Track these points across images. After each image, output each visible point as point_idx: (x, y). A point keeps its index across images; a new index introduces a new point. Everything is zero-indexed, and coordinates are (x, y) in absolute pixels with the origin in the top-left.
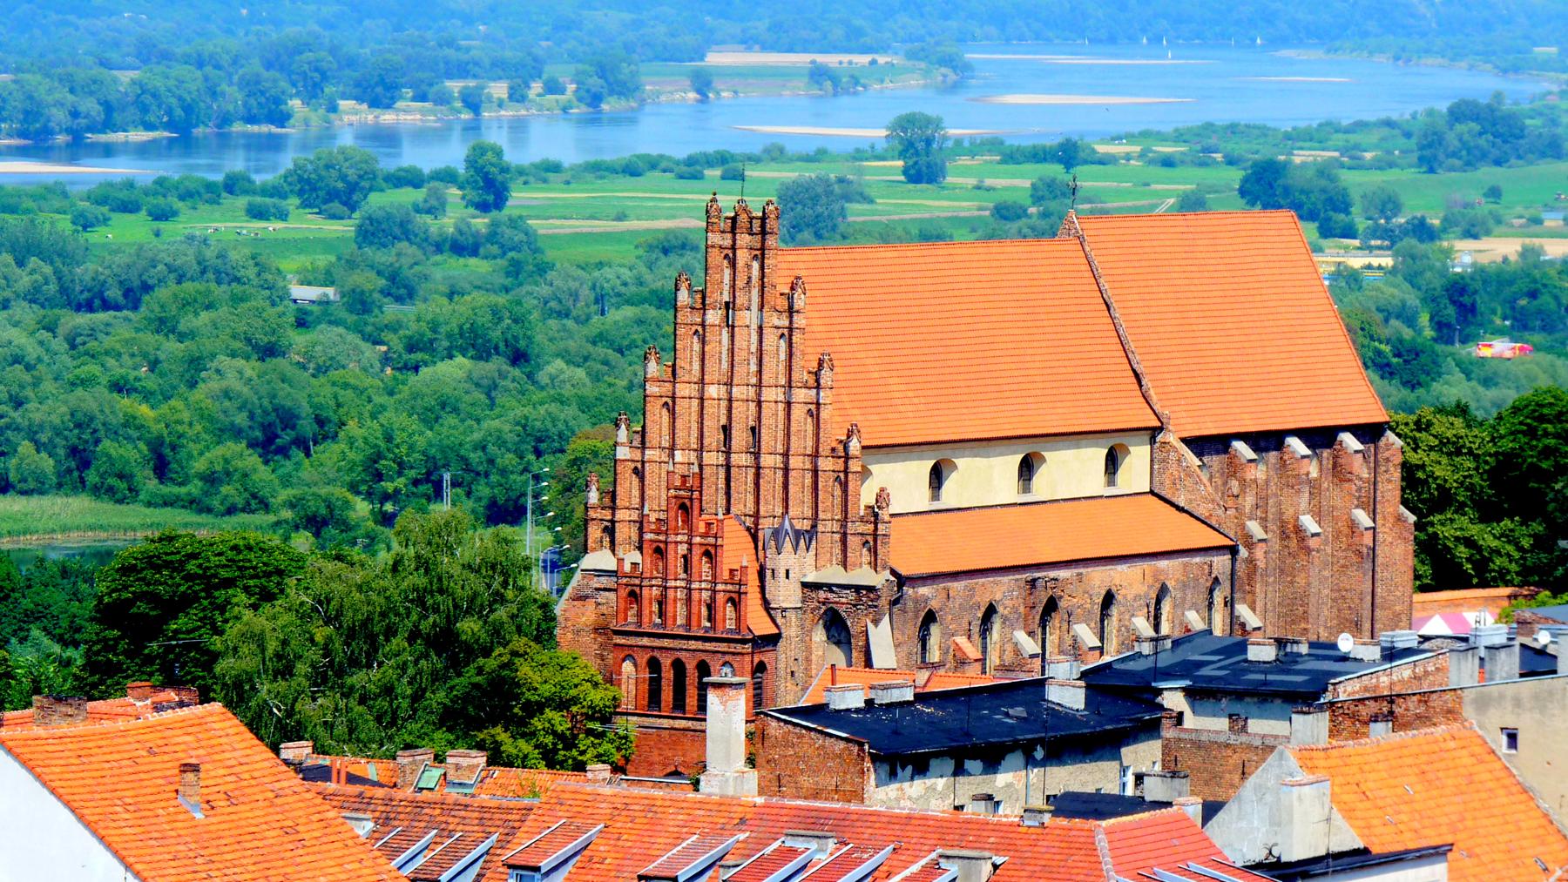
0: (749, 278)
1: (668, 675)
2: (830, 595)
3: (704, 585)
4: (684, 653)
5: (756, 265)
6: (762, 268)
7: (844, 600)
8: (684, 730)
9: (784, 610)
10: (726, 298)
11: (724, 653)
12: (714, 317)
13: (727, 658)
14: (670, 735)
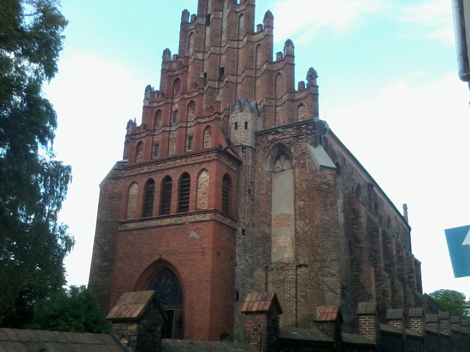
2: (276, 136)
4: (172, 171)
7: (288, 136)
9: (244, 147)
10: (209, 12)
13: (204, 166)
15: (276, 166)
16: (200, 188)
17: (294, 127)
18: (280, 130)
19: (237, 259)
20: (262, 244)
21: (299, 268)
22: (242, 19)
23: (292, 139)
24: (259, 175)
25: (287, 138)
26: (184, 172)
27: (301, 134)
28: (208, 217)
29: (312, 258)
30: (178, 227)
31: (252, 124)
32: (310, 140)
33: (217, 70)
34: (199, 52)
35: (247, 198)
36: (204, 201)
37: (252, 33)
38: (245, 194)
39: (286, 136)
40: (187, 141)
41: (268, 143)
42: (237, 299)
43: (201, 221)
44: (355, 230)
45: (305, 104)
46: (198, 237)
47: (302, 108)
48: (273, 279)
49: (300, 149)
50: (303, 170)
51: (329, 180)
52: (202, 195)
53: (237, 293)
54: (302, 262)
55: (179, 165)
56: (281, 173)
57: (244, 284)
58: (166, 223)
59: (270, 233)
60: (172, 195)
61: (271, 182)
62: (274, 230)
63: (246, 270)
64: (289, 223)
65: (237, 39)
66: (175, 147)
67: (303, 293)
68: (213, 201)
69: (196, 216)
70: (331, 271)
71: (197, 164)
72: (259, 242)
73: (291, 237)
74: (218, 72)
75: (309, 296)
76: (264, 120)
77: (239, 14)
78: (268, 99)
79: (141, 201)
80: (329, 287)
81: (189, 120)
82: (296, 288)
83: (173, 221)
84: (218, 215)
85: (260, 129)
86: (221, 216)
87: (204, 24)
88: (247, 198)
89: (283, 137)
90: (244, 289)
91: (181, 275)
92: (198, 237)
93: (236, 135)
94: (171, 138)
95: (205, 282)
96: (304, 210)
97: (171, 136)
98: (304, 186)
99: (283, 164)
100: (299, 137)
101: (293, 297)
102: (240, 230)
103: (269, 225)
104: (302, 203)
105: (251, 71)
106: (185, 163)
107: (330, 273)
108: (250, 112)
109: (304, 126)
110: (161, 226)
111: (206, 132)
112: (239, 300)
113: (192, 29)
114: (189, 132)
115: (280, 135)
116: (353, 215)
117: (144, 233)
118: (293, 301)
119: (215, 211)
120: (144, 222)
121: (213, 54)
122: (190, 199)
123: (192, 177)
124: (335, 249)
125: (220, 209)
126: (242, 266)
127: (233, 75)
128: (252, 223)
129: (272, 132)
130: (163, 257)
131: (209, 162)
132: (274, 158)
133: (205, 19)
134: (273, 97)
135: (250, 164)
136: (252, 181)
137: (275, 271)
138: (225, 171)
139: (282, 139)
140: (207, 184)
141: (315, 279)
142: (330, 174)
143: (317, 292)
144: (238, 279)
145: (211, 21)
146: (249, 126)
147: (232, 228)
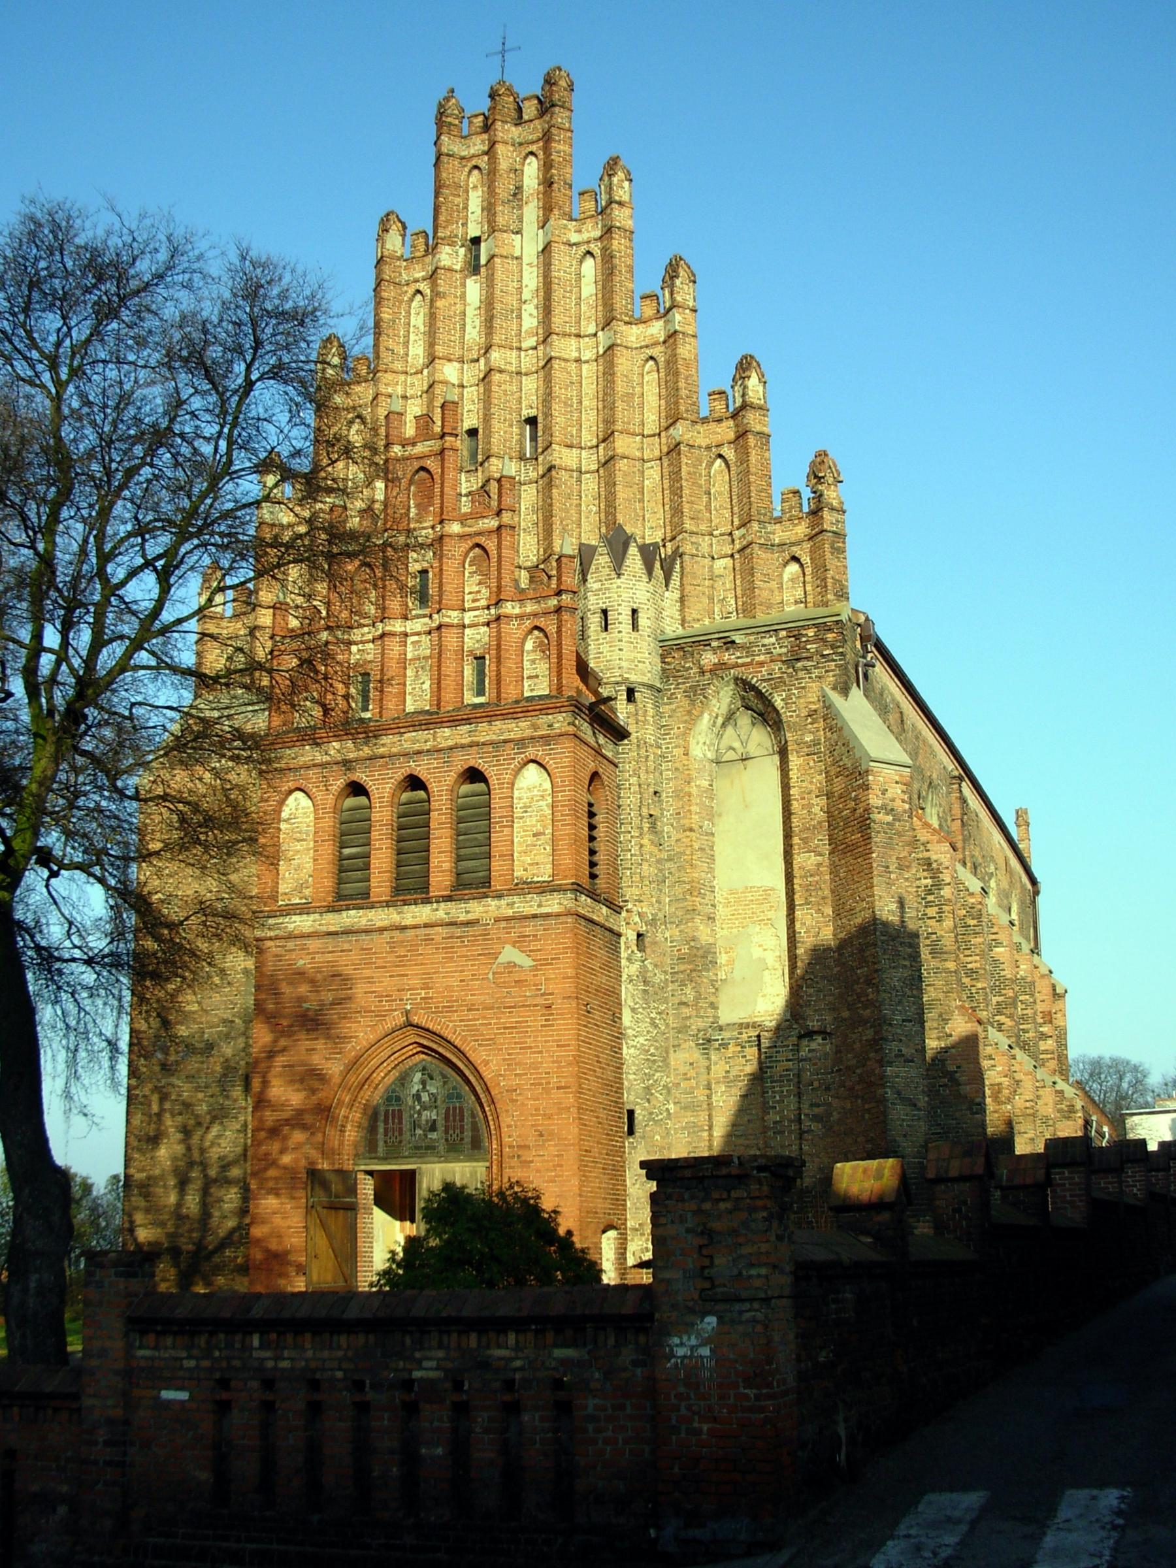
0: (519, 189)
1: (383, 815)
2: (728, 657)
3: (468, 618)
4: (424, 760)
5: (531, 171)
6: (547, 165)
7: (762, 658)
8: (426, 926)
10: (473, 231)
11: (521, 743)
12: (452, 257)
13: (531, 752)
14: (393, 945)
15: (725, 743)
16: (521, 818)
17: (783, 633)
18: (738, 638)
19: (627, 1018)
20: (694, 974)
21: (805, 1042)
22: (589, 266)
23: (776, 666)
24: (677, 769)
25: (761, 664)
26: (466, 767)
27: (804, 655)
28: (554, 904)
29: (846, 1014)
30: (458, 931)
31: (651, 613)
32: (831, 674)
33: (511, 426)
34: (450, 360)
35: (645, 841)
36: (538, 859)
37: (627, 319)
38: (642, 828)
39: (757, 658)
40: (469, 672)
41: (703, 673)
42: (631, 1132)
43: (535, 916)
44: (932, 922)
45: (806, 559)
46: (526, 961)
47: (794, 568)
48: (728, 1072)
49: (802, 701)
50: (812, 764)
51: (893, 800)
52: (530, 840)
53: (631, 1113)
54: (814, 1024)
55: (450, 743)
56: (741, 764)
57: (648, 1088)
58: (418, 921)
59: (711, 940)
60: (434, 834)
61: (710, 792)
62: (725, 932)
63: (652, 1050)
64: (771, 914)
65: (573, 330)
66: (426, 686)
67: (816, 1110)
68: (567, 860)
69: (516, 899)
70: (904, 1051)
71: (512, 745)
72: (682, 968)
73: (778, 954)
74: (515, 430)
75: (836, 1116)
76: (682, 600)
77: (583, 248)
78: (692, 533)
79: (328, 851)
80: (899, 1093)
81: (467, 606)
82: (799, 1095)
83: (441, 914)
84: (583, 897)
85: (673, 629)
86: (589, 900)
87: (458, 267)
88: (645, 841)
89: (749, 660)
90: (648, 1101)
91: (482, 1069)
92: (526, 962)
93: (605, 648)
94: (409, 656)
95: (558, 1088)
96: (817, 878)
97: (410, 648)
98: (816, 810)
99: (744, 738)
100: (799, 665)
101: (791, 1121)
102: (632, 936)
103: (709, 918)
104: (813, 859)
105: (628, 439)
106: (469, 739)
107: (900, 1055)
108: (645, 578)
109: (811, 633)
110: (404, 928)
111: (529, 645)
112: (637, 1134)
113: (416, 281)
114: (469, 644)
115: (738, 654)
116: (926, 878)
117: (346, 946)
118: (790, 1132)
119: (578, 889)
120: (344, 914)
121: (501, 371)
122: (494, 852)
123: (493, 781)
124: (911, 990)
125: (585, 881)
126: (641, 1040)
127: (570, 446)
128: (661, 915)
129: (714, 644)
130: (415, 1020)
131: (546, 740)
132: (720, 720)
133: (462, 251)
134: (703, 527)
135: (651, 739)
136: (659, 789)
137: (732, 1049)
138: (592, 766)
139: (743, 665)
140: (545, 808)
141: (858, 1071)
142: (897, 783)
143: (867, 1106)
144: (631, 1077)
145: (483, 261)
146: (643, 621)
147: (611, 930)
